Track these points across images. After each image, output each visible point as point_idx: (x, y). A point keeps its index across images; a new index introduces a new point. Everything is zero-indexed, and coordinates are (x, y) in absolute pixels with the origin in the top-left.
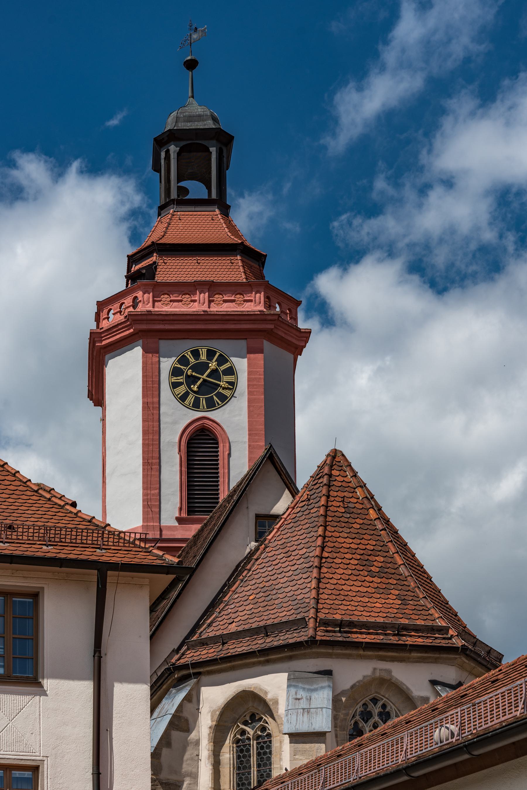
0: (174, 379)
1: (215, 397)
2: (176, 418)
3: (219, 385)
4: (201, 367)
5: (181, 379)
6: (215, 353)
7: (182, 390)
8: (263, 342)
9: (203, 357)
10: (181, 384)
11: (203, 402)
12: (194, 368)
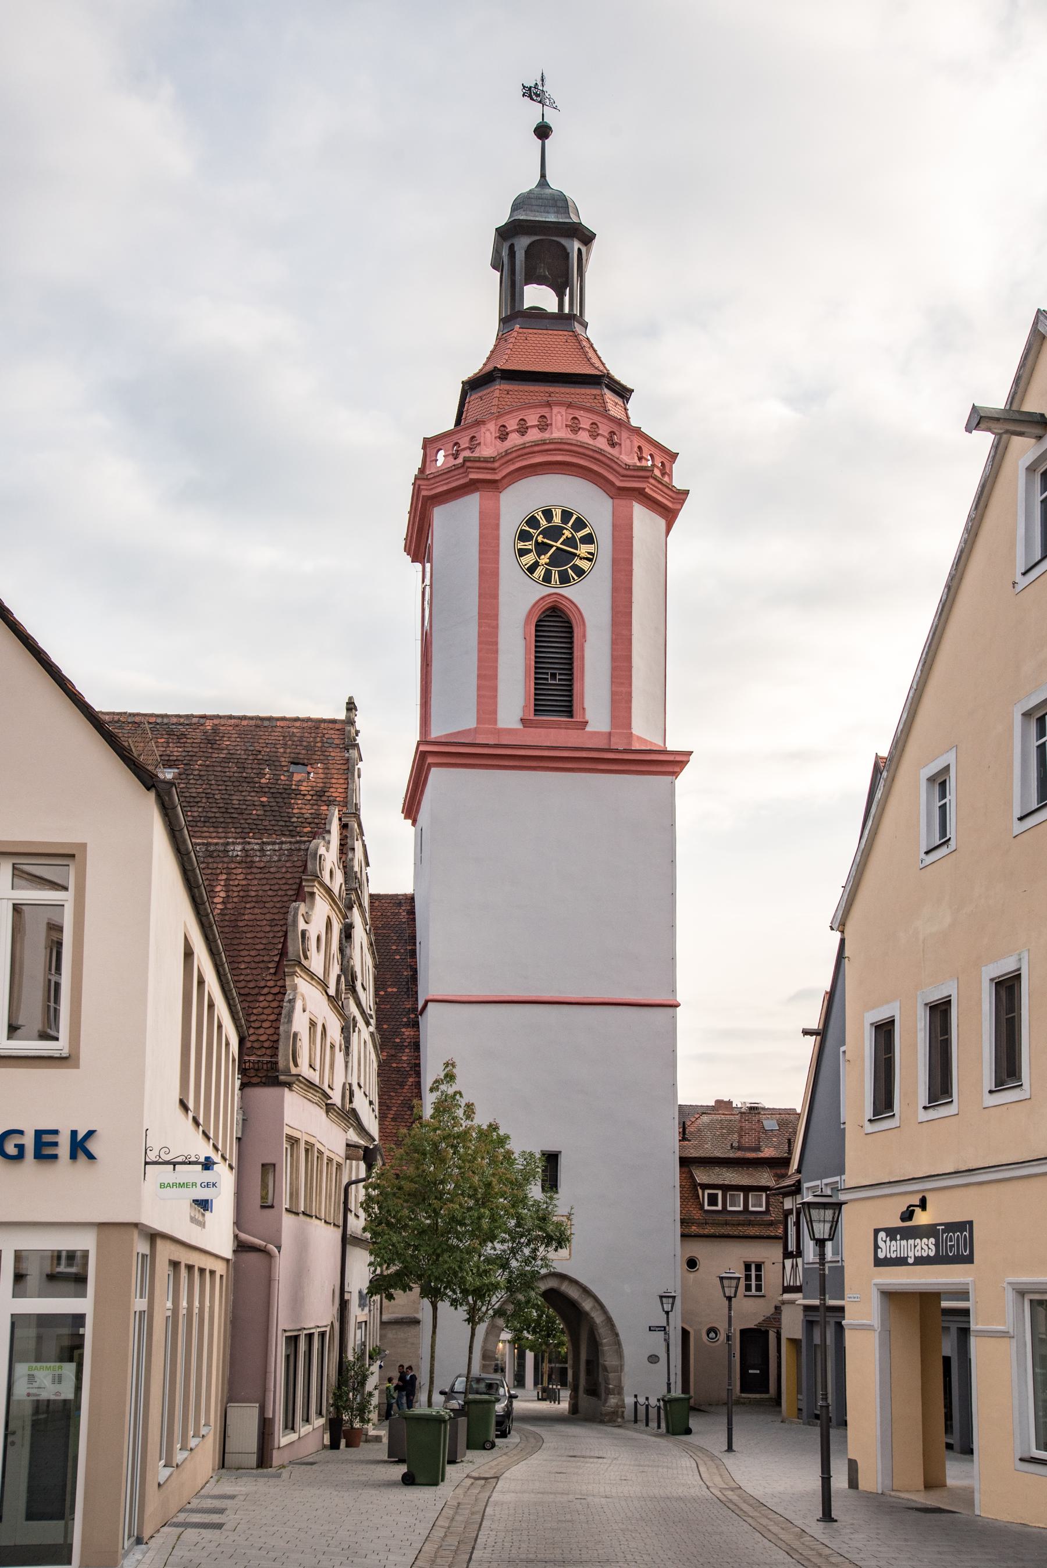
0: (521, 545)
1: (570, 571)
2: (521, 595)
3: (575, 555)
4: (554, 532)
5: (529, 545)
6: (571, 514)
7: (529, 559)
8: (632, 507)
9: (557, 520)
10: (529, 551)
11: (555, 577)
12: (545, 533)
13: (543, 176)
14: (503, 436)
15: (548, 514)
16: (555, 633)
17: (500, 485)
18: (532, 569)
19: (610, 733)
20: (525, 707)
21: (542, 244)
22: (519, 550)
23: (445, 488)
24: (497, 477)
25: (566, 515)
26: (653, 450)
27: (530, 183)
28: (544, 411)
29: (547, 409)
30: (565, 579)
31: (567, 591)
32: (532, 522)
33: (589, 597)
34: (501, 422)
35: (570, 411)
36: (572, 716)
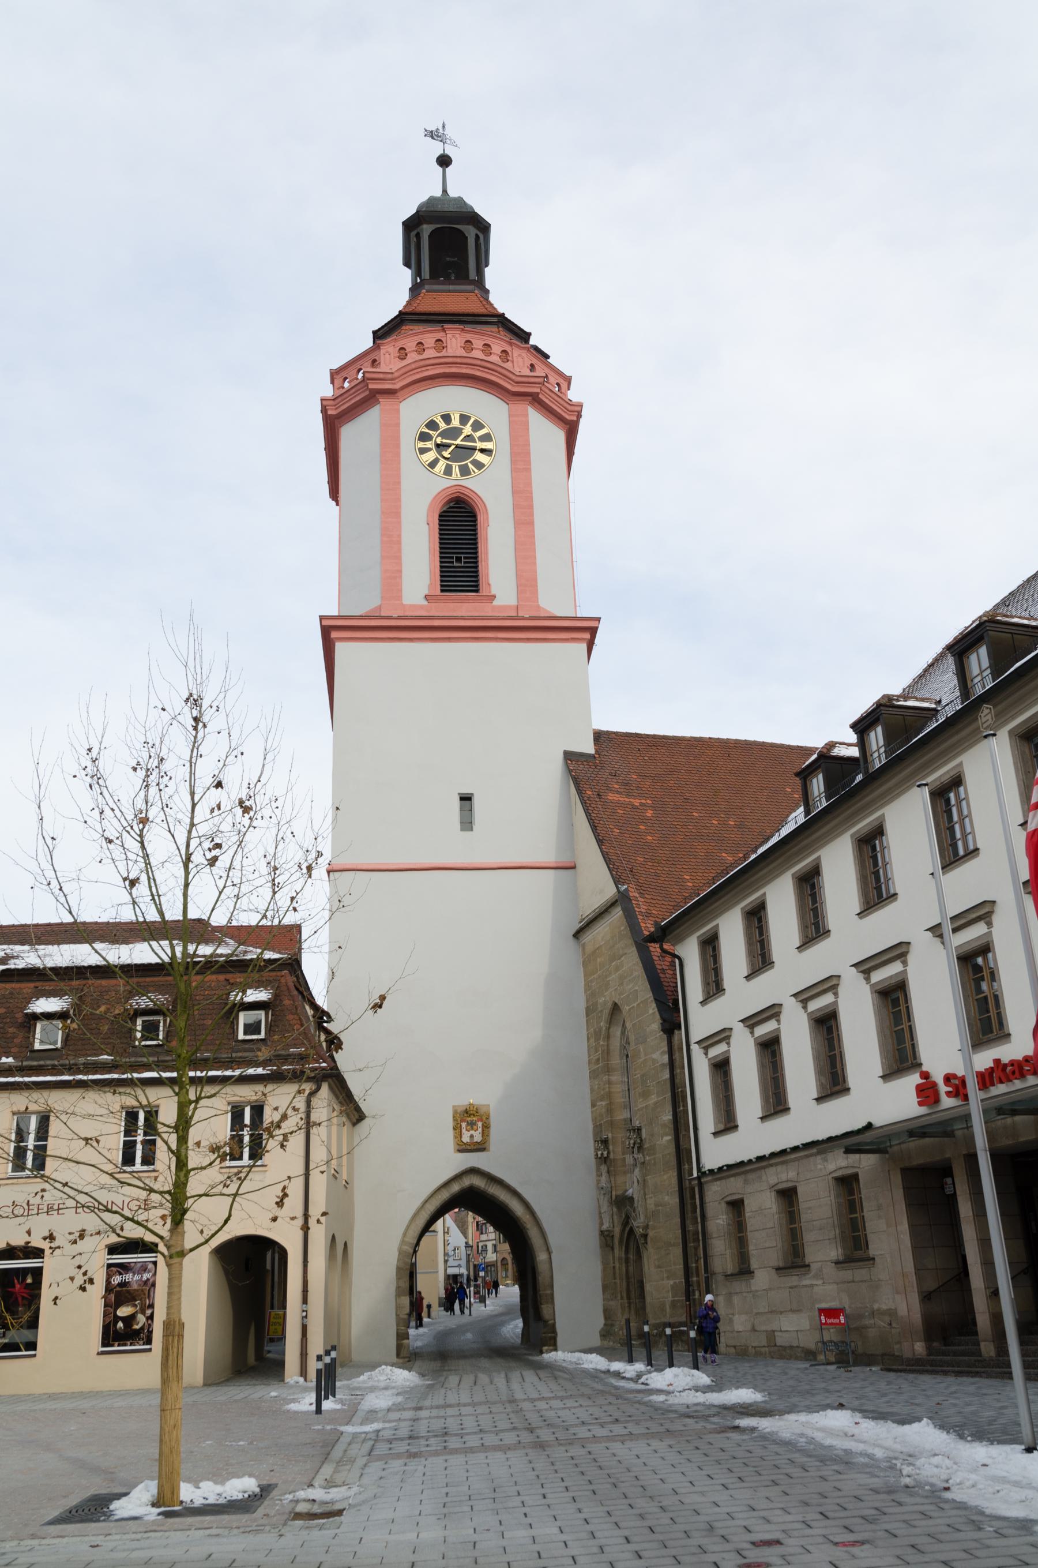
0: (421, 445)
1: (470, 465)
2: (423, 488)
3: (474, 449)
4: (454, 433)
5: (429, 444)
6: (470, 418)
8: (527, 410)
9: (456, 422)
12: (444, 434)
15: (447, 418)
17: (398, 394)
18: (433, 464)
21: (446, 243)
22: (420, 449)
24: (397, 386)
25: (464, 419)
31: (469, 483)
33: (490, 487)
36: (477, 591)
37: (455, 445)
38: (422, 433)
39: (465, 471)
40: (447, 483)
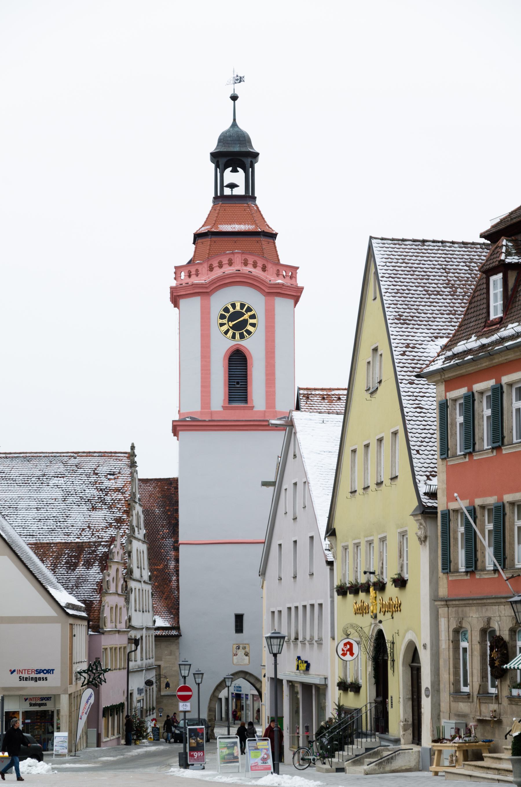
0: (221, 321)
1: (245, 333)
2: (222, 344)
5: (225, 321)
6: (245, 305)
7: (225, 328)
9: (238, 308)
10: (225, 324)
11: (237, 336)
13: (234, 120)
14: (211, 269)
15: (234, 306)
16: (238, 361)
18: (226, 332)
19: (265, 411)
20: (224, 400)
21: (234, 154)
22: (220, 324)
23: (184, 293)
25: (242, 306)
26: (285, 268)
27: (227, 125)
28: (231, 256)
29: (232, 255)
30: (242, 336)
32: (226, 310)
33: (254, 345)
34: (210, 263)
35: (243, 255)
37: (238, 321)
38: (221, 314)
39: (242, 336)
40: (233, 343)
